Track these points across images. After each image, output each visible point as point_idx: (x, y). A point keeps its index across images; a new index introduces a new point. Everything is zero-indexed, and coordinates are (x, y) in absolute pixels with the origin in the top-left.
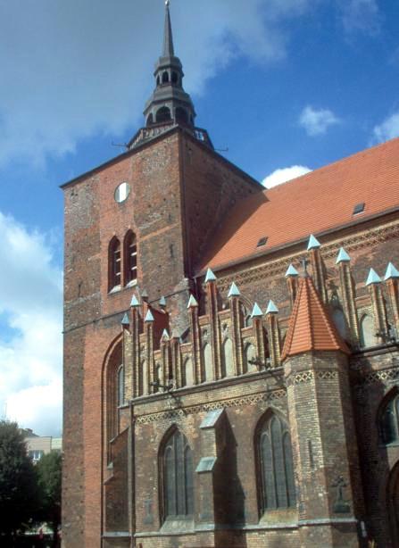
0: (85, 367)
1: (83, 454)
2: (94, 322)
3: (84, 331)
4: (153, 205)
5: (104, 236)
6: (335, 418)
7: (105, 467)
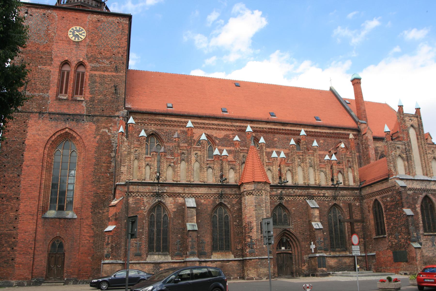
0: (27, 142)
1: (19, 205)
2: (39, 113)
4: (103, 54)
5: (57, 56)
7: (40, 216)
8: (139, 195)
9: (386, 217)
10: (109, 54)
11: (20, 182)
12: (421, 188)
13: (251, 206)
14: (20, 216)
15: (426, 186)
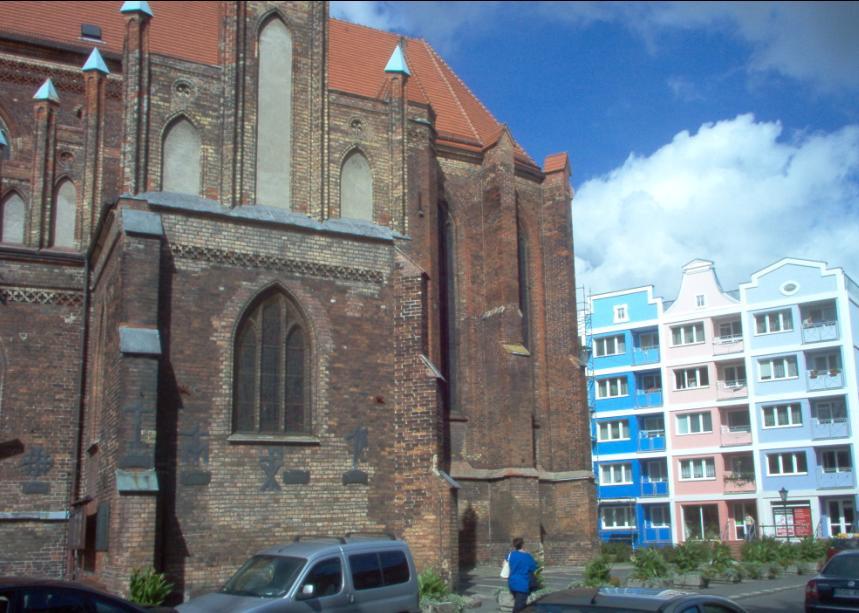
12: (257, 256)
15: (283, 248)
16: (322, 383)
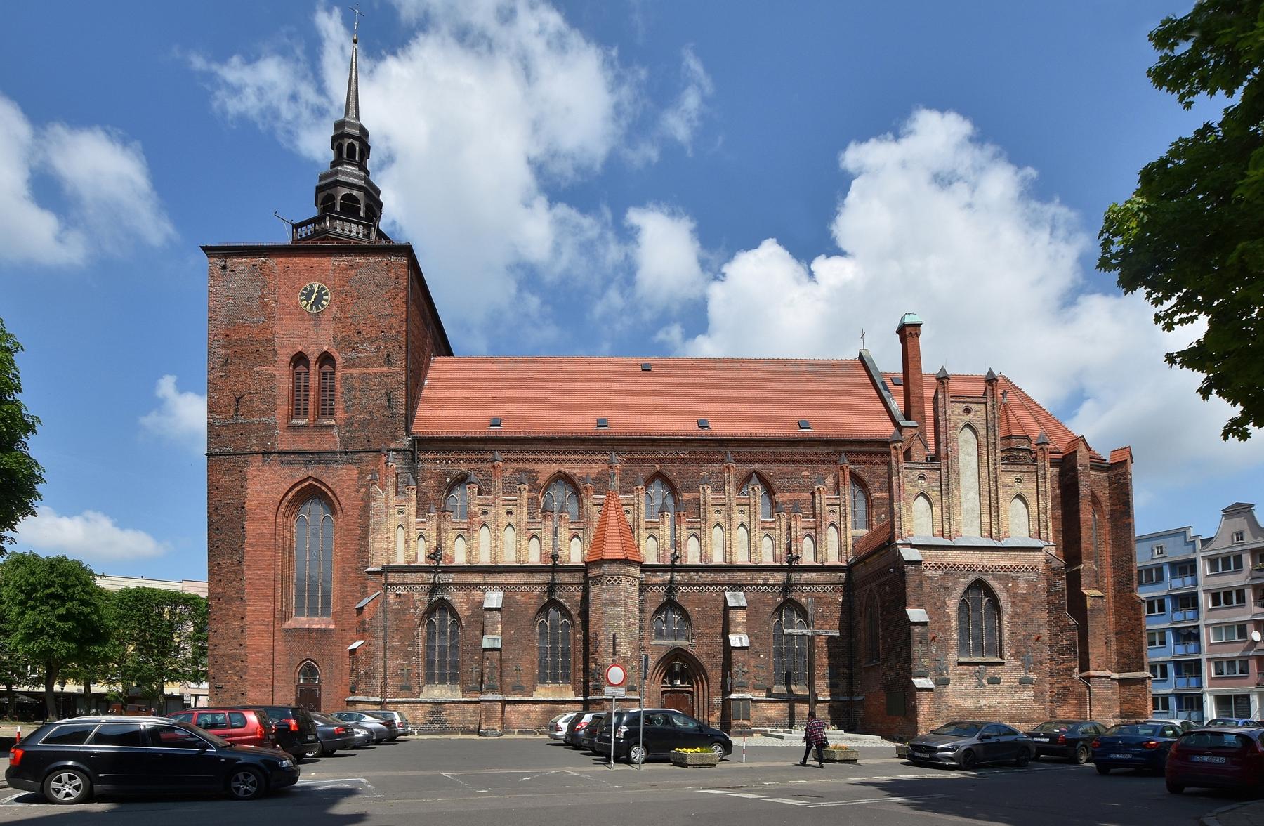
0: (247, 505)
3: (246, 461)
4: (364, 332)
5: (283, 346)
6: (634, 618)
8: (405, 589)
9: (882, 626)
10: (373, 333)
11: (243, 572)
13: (598, 604)
14: (249, 628)
16: (1006, 631)
